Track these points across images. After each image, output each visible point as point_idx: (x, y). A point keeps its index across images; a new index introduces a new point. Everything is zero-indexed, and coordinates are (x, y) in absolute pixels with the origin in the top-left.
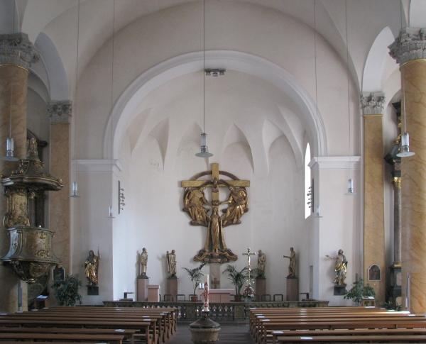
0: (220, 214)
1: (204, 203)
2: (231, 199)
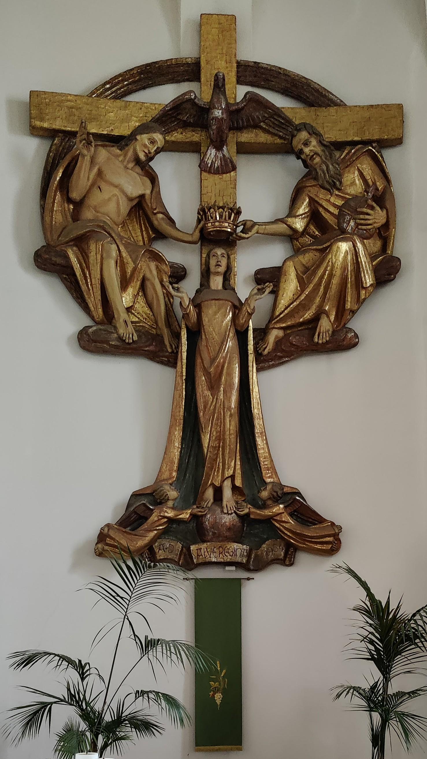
0: (244, 290)
1: (160, 236)
2: (303, 209)
